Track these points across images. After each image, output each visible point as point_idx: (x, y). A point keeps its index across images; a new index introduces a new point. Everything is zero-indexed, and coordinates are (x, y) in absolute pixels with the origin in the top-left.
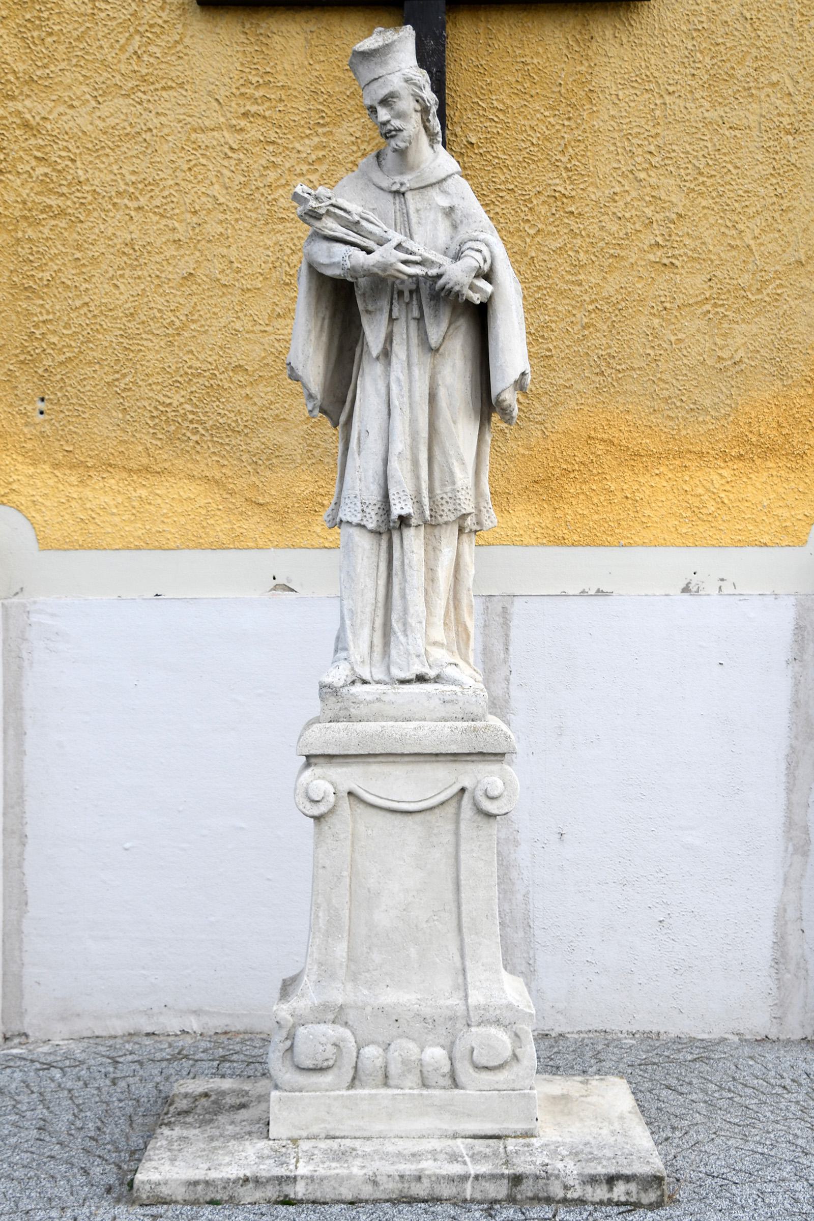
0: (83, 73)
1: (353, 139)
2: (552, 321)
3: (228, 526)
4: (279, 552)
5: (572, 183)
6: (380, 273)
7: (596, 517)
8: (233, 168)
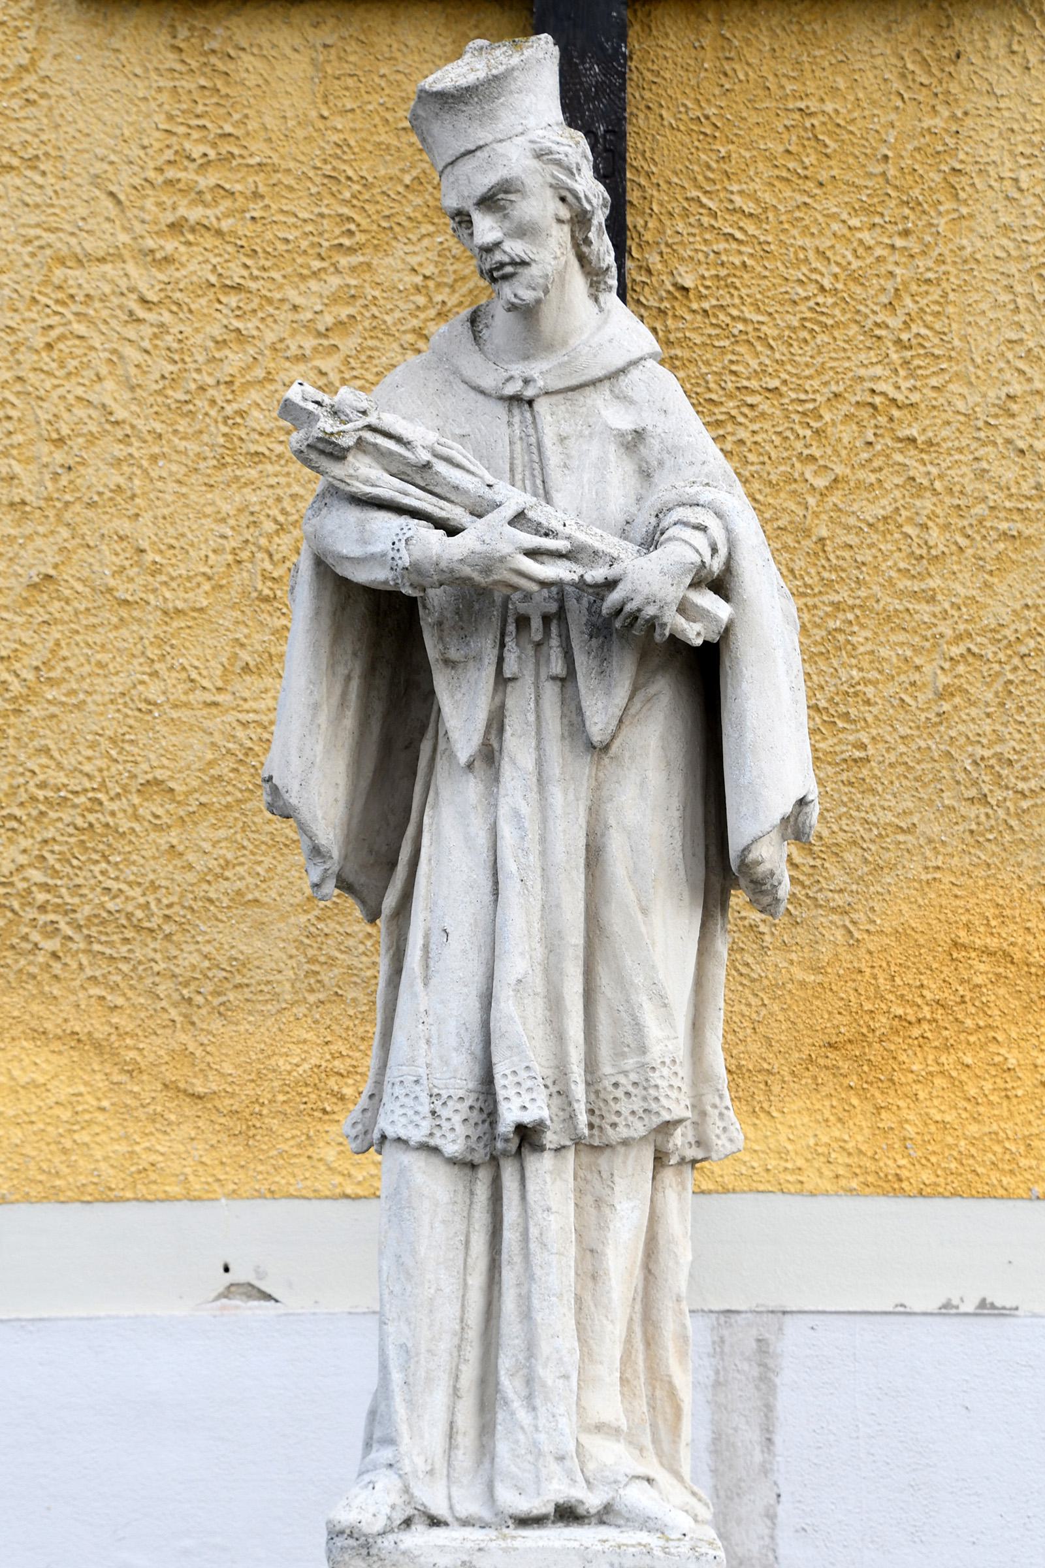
1: (418, 279)
2: (867, 681)
3: (122, 1148)
4: (238, 1205)
5: (911, 375)
6: (477, 577)
7: (973, 1129)
8: (146, 344)
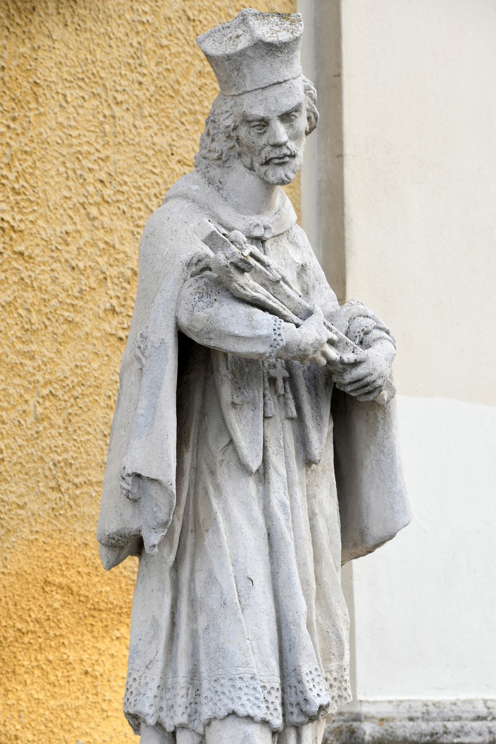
5: (21, 212)
7: (52, 703)
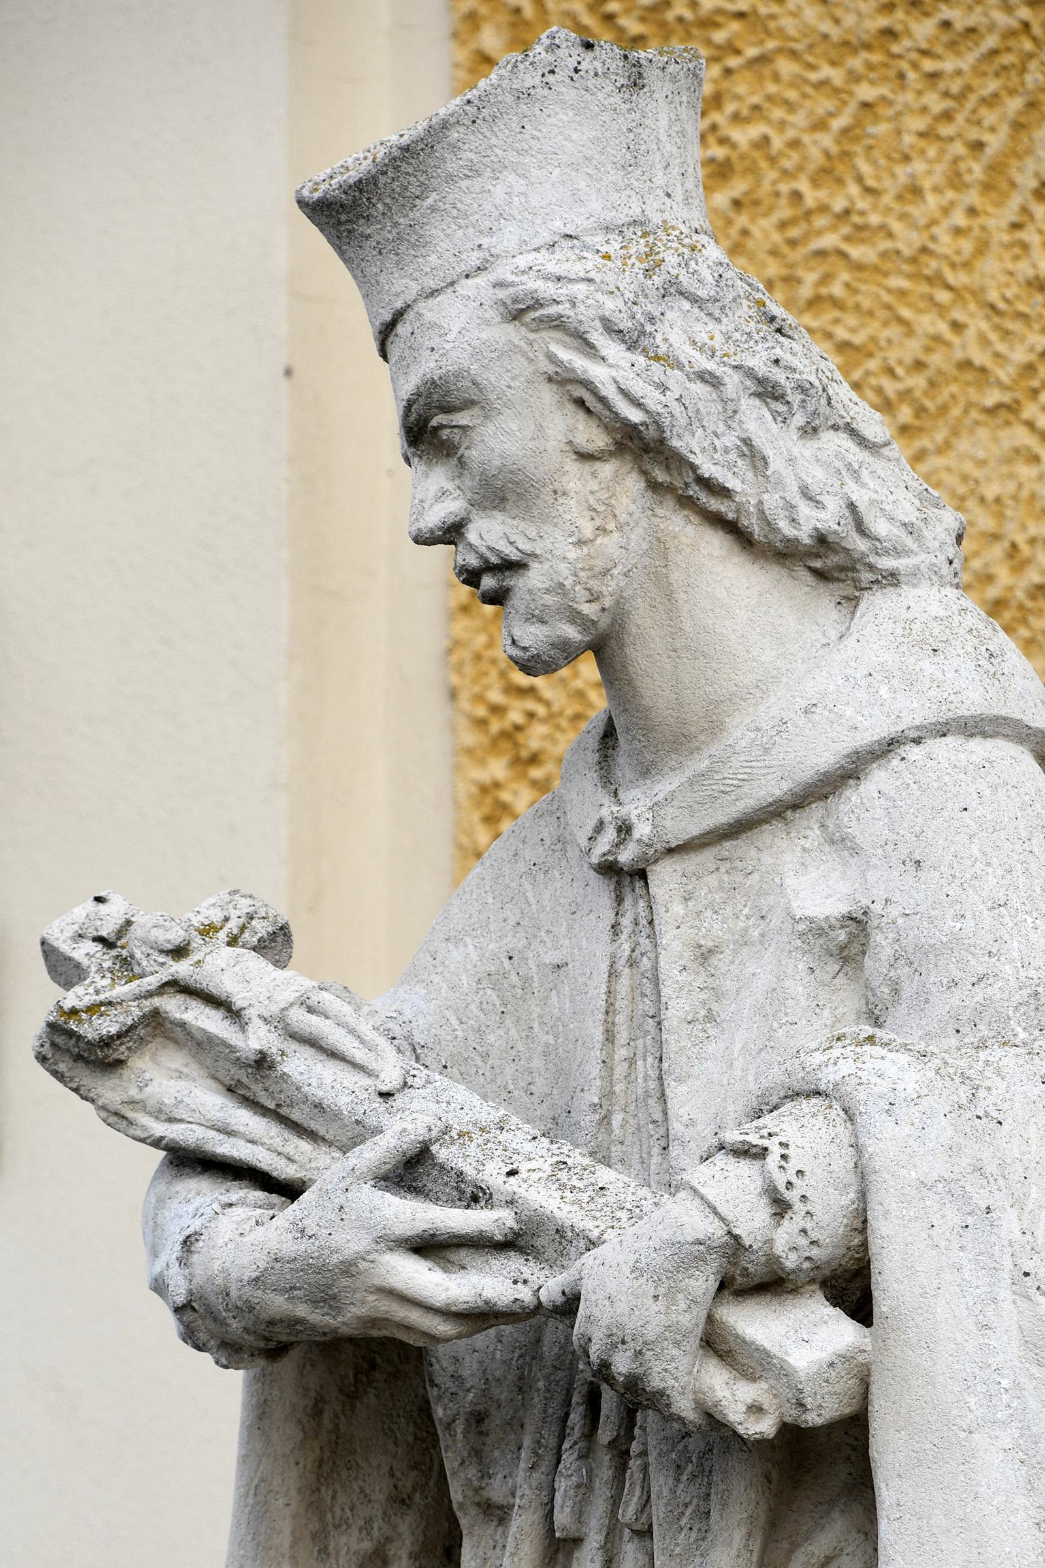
0: (841, 333)
6: (316, 1317)
